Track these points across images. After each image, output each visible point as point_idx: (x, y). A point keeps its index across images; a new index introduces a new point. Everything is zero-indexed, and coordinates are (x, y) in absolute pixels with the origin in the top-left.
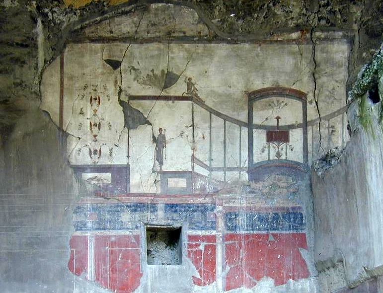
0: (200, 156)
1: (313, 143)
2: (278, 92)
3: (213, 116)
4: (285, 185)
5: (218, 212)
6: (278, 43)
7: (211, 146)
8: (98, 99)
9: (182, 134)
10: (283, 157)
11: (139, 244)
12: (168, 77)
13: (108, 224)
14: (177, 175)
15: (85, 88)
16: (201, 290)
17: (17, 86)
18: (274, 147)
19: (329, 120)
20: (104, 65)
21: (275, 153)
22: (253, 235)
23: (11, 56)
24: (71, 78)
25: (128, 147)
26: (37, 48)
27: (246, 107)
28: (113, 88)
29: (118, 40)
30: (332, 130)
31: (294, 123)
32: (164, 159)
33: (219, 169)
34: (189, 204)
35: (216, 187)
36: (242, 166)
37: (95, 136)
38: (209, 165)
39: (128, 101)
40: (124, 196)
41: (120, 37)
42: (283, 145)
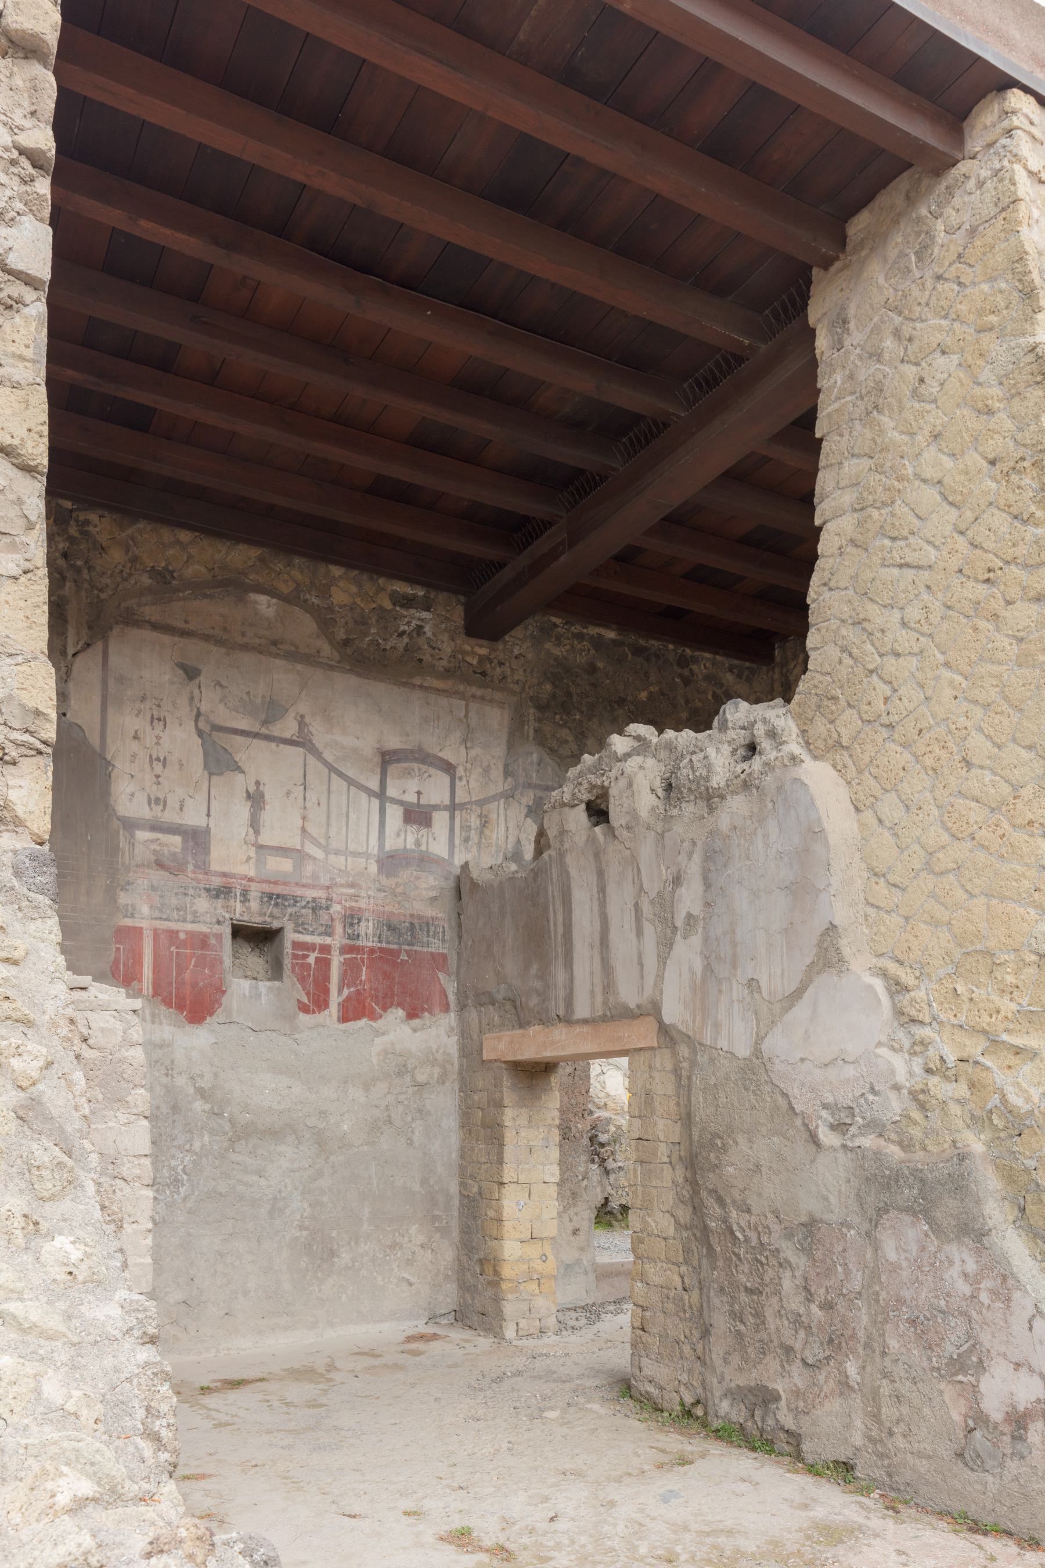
0: (312, 830)
2: (422, 757)
3: (333, 776)
4: (425, 886)
7: (328, 817)
8: (162, 720)
9: (288, 793)
10: (423, 848)
19: (481, 806)
22: (381, 949)
24: (121, 679)
26: (66, 621)
27: (378, 771)
30: (486, 822)
31: (438, 802)
33: (337, 853)
37: (158, 776)
42: (424, 831)
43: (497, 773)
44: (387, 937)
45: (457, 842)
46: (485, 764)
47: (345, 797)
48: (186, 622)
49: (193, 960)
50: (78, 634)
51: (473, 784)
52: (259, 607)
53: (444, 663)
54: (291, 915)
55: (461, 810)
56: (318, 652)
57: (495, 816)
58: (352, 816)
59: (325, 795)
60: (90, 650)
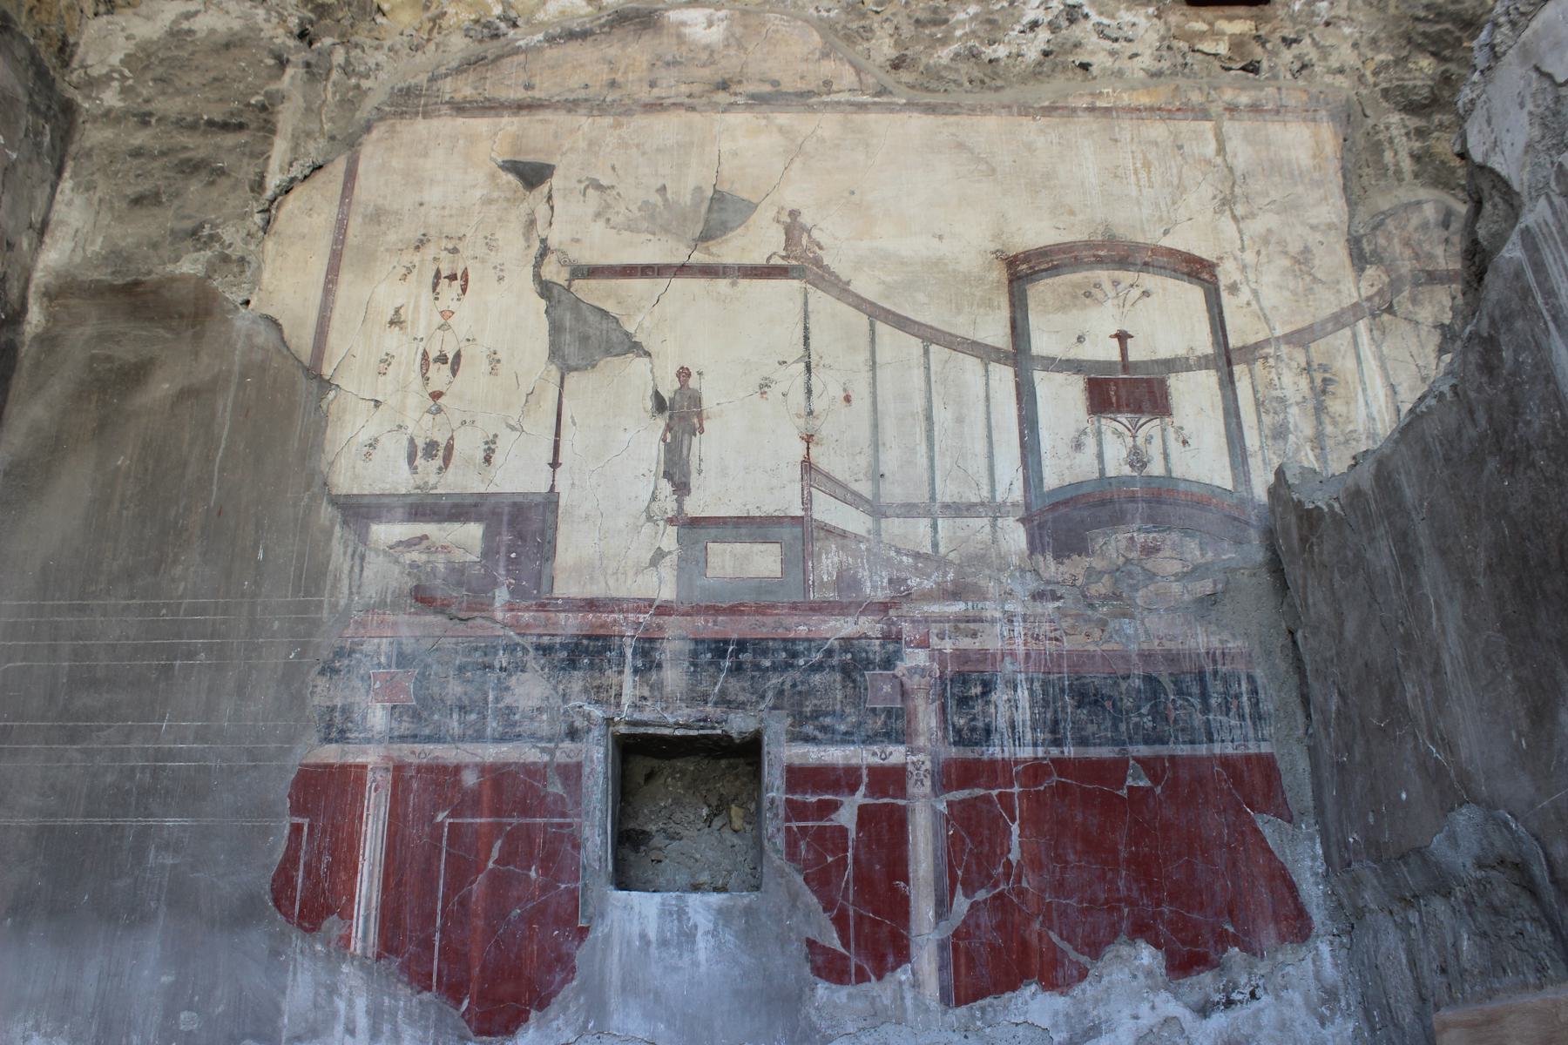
1: (1260, 421)
3: (881, 327)
4: (1176, 567)
5: (912, 671)
6: (1097, 113)
7: (875, 426)
9: (764, 387)
10: (1156, 468)
11: (578, 803)
12: (715, 207)
13: (455, 716)
14: (743, 531)
15: (420, 245)
16: (844, 1000)
17: (183, 239)
18: (1120, 435)
20: (493, 177)
21: (1124, 454)
22: (1061, 764)
23: (183, 156)
25: (558, 434)
26: (273, 132)
27: (1004, 301)
28: (521, 243)
29: (547, 107)
30: (1325, 380)
32: (694, 475)
33: (909, 510)
34: (793, 641)
35: (903, 575)
36: (999, 499)
37: (436, 396)
38: (870, 497)
39: (570, 281)
40: (527, 609)
41: (557, 98)
42: (1152, 427)
43: (1333, 257)
44: (1078, 727)
45: (1252, 440)
46: (1295, 248)
47: (917, 376)
48: (528, 87)
49: (498, 843)
50: (295, 148)
51: (1270, 297)
52: (687, 31)
53: (1146, 60)
54: (781, 693)
55: (1248, 363)
56: (827, 83)
57: (1350, 363)
58: (942, 416)
59: (865, 375)
60: (320, 176)
